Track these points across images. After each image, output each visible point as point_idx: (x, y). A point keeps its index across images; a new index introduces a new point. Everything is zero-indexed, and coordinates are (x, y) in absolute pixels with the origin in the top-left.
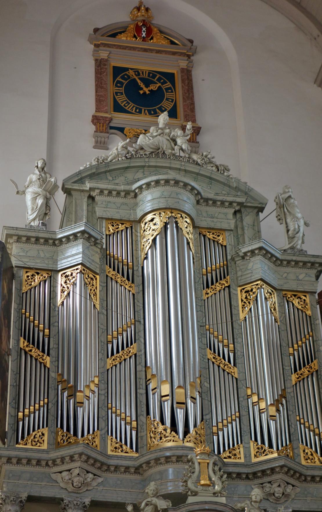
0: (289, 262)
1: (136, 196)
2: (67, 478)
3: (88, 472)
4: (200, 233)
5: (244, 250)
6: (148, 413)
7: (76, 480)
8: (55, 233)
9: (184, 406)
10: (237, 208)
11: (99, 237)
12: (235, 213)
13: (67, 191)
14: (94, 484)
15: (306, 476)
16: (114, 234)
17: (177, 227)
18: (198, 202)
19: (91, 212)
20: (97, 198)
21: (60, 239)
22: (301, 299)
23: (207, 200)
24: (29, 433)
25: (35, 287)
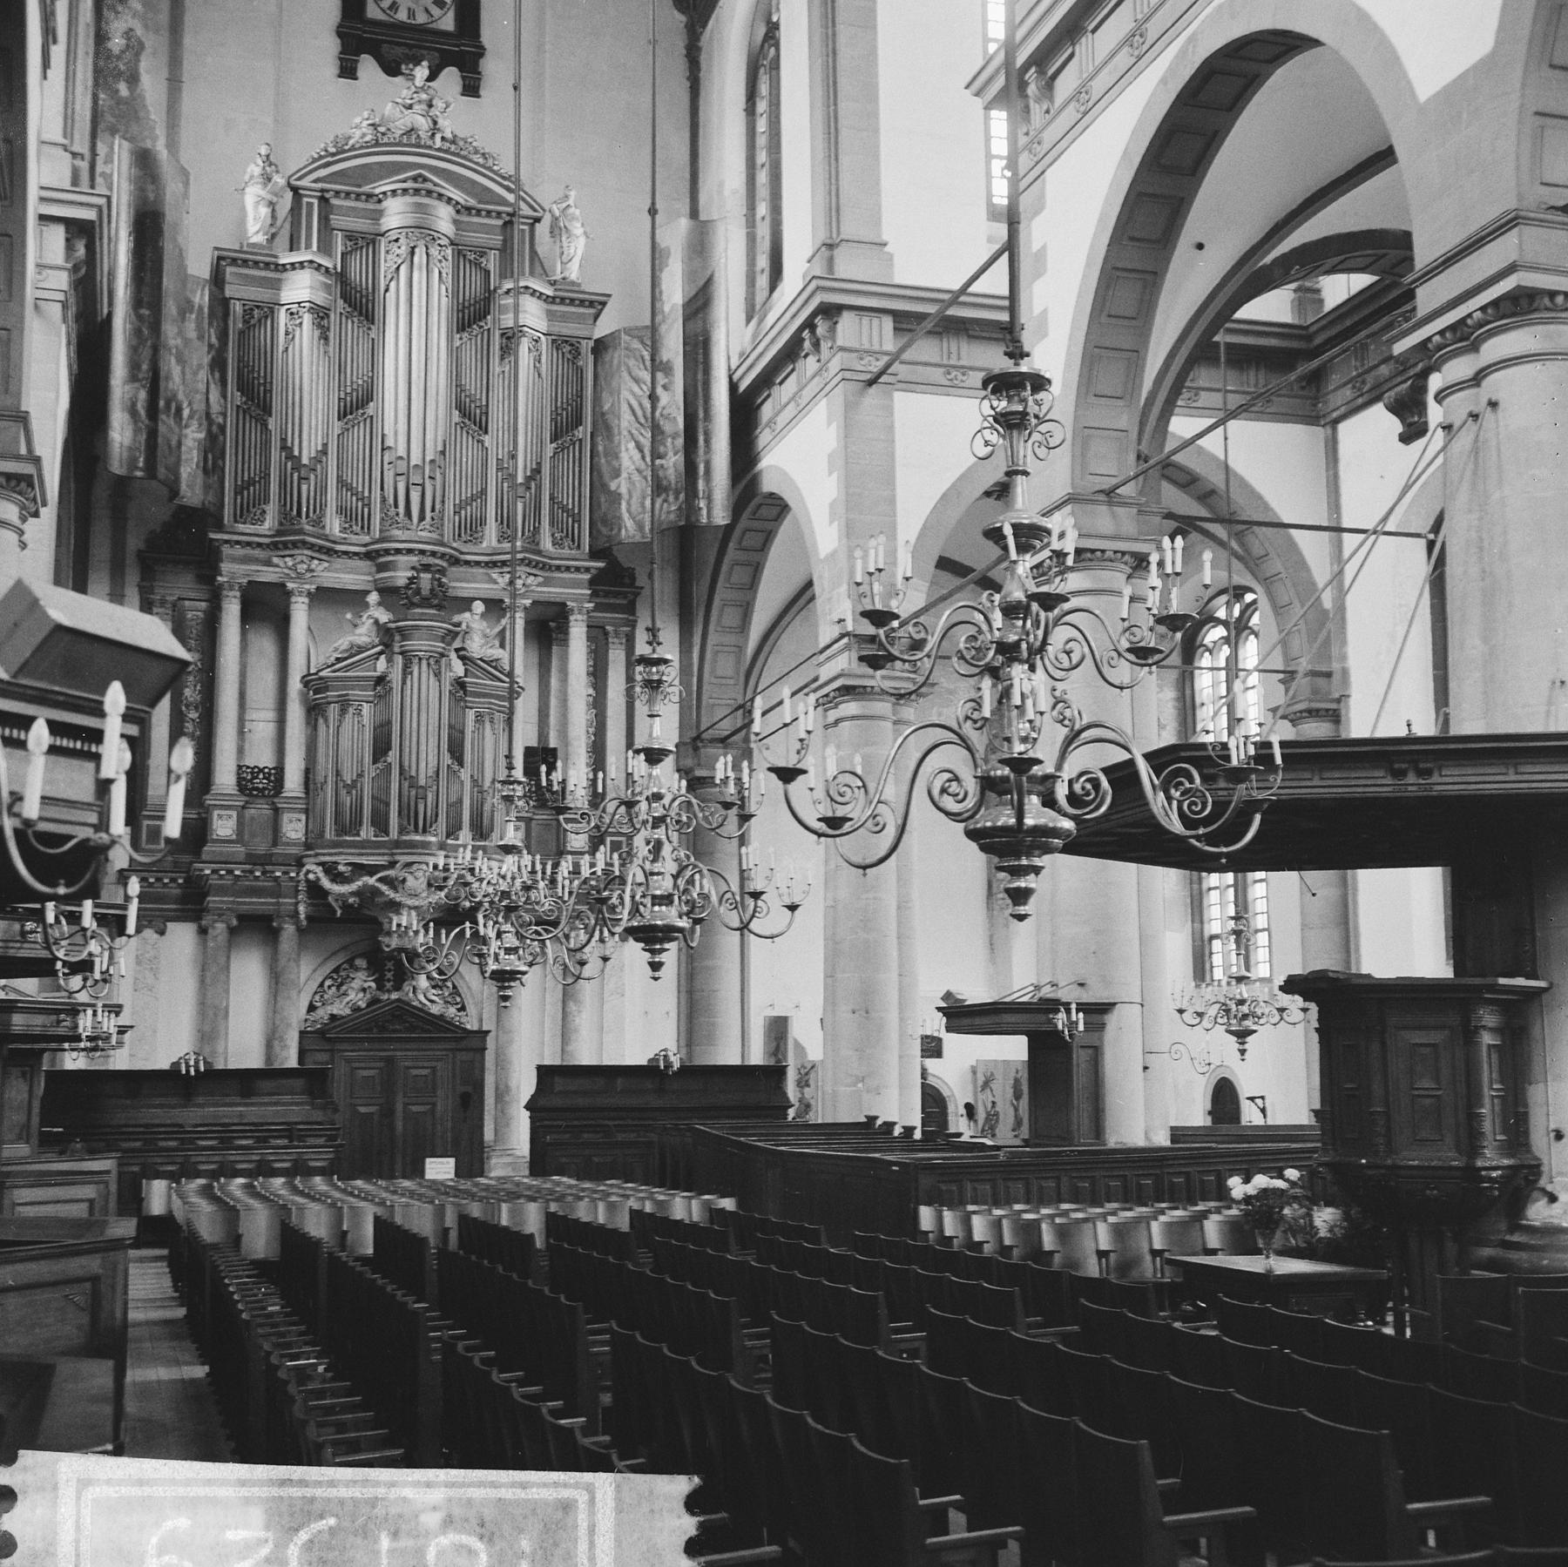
0: (563, 300)
1: (380, 201)
2: (290, 564)
3: (313, 558)
4: (459, 252)
5: (508, 285)
6: (382, 489)
7: (299, 566)
8: (276, 257)
9: (419, 488)
10: (508, 218)
11: (330, 265)
12: (506, 223)
13: (295, 190)
14: (321, 568)
15: (550, 566)
16: (351, 252)
17: (427, 254)
18: (458, 212)
19: (324, 220)
20: (335, 202)
21: (284, 265)
22: (572, 345)
23: (468, 209)
24: (248, 511)
25: (254, 326)
